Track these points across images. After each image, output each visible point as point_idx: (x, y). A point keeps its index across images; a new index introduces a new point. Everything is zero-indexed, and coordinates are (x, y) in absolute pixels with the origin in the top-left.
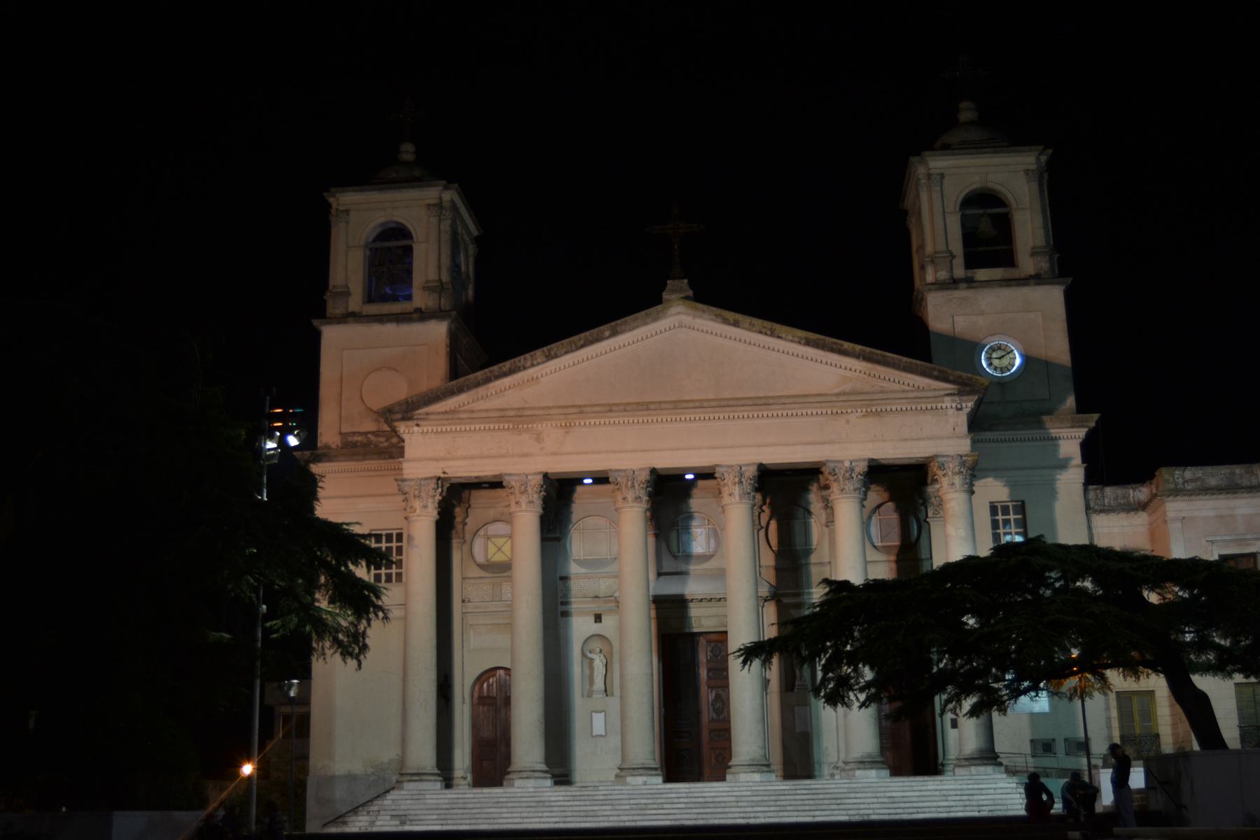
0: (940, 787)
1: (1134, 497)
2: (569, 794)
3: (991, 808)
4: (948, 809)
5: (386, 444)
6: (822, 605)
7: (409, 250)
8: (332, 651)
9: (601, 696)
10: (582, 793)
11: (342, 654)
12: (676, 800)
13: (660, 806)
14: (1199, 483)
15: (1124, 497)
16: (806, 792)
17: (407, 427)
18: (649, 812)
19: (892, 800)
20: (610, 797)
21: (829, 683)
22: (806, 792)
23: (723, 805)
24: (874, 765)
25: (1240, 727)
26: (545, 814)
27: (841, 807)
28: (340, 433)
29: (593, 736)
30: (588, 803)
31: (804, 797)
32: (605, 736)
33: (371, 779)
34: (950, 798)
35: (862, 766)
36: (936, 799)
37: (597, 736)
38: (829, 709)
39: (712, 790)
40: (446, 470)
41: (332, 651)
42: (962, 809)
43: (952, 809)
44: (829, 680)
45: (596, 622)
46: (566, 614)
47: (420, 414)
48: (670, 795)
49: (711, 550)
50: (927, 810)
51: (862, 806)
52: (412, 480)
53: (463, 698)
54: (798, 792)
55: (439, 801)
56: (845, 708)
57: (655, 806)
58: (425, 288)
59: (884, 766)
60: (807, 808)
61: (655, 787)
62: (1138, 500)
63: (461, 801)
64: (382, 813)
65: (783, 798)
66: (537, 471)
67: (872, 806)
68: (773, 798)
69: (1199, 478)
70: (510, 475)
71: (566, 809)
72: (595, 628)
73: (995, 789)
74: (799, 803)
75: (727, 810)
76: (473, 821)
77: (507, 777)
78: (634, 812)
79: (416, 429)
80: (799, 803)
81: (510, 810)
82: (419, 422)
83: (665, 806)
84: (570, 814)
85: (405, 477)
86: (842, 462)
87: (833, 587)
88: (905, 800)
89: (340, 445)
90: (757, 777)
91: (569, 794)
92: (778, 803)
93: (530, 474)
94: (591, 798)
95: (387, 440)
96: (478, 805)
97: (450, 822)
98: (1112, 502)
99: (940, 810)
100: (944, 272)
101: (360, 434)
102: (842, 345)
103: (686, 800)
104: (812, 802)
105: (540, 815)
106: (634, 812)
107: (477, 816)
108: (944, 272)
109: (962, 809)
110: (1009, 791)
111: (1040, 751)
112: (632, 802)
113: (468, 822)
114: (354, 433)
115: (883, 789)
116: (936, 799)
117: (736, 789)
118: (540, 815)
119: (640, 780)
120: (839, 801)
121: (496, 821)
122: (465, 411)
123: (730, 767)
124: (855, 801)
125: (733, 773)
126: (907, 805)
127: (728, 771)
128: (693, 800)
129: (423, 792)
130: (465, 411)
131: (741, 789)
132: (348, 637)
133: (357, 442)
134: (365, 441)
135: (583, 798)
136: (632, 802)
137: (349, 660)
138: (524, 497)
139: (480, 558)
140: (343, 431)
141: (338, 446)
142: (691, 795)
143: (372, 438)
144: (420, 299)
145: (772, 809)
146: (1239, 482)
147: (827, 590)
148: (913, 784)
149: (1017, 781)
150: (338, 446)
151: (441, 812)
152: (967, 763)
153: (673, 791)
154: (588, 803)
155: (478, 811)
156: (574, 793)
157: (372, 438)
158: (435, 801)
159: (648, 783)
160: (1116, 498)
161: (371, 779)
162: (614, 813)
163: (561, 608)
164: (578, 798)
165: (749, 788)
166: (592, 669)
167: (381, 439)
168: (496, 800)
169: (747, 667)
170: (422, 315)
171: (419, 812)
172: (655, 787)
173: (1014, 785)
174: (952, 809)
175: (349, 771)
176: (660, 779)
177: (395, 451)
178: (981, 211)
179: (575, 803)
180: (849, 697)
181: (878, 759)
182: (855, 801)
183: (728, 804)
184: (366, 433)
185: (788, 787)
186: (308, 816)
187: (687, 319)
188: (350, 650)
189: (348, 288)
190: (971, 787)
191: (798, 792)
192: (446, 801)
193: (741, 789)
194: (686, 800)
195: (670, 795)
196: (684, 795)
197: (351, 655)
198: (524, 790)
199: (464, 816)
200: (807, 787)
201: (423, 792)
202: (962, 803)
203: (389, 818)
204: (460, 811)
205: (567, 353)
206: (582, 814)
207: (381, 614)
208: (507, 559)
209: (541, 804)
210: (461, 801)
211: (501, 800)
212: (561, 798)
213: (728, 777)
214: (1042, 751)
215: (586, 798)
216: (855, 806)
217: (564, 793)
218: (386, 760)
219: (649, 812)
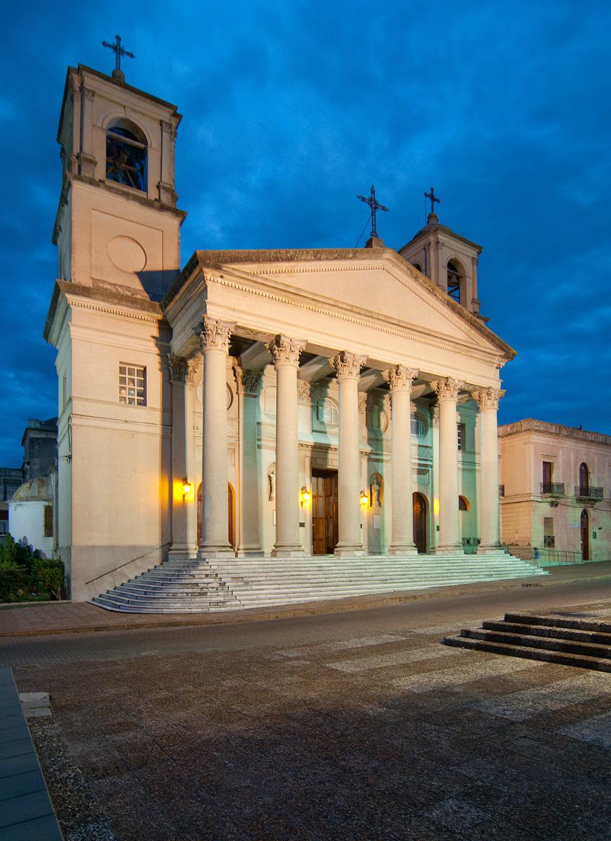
17: (213, 275)
46: (259, 447)
47: (228, 267)
70: (285, 337)
79: (220, 280)
82: (224, 275)
93: (297, 340)
95: (133, 295)
101: (110, 284)
102: (463, 311)
122: (262, 278)
130: (262, 278)
163: (258, 443)
187: (388, 265)
205: (327, 259)
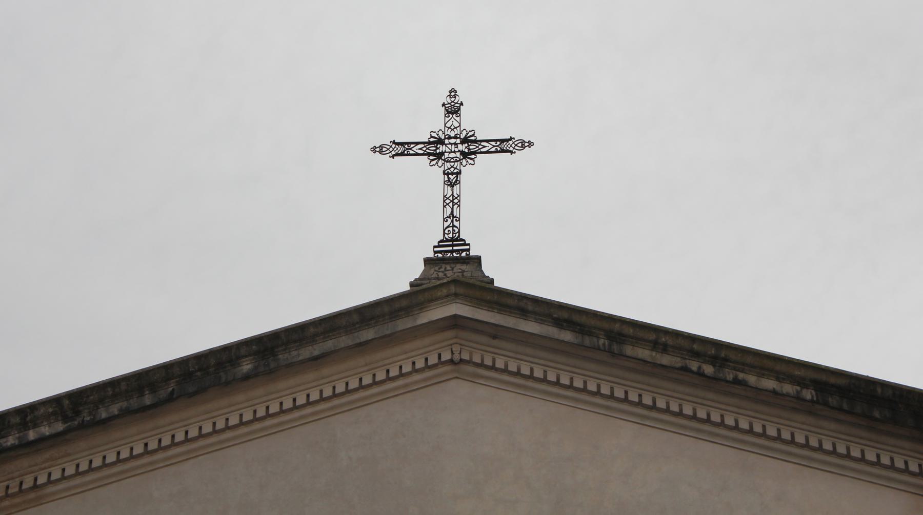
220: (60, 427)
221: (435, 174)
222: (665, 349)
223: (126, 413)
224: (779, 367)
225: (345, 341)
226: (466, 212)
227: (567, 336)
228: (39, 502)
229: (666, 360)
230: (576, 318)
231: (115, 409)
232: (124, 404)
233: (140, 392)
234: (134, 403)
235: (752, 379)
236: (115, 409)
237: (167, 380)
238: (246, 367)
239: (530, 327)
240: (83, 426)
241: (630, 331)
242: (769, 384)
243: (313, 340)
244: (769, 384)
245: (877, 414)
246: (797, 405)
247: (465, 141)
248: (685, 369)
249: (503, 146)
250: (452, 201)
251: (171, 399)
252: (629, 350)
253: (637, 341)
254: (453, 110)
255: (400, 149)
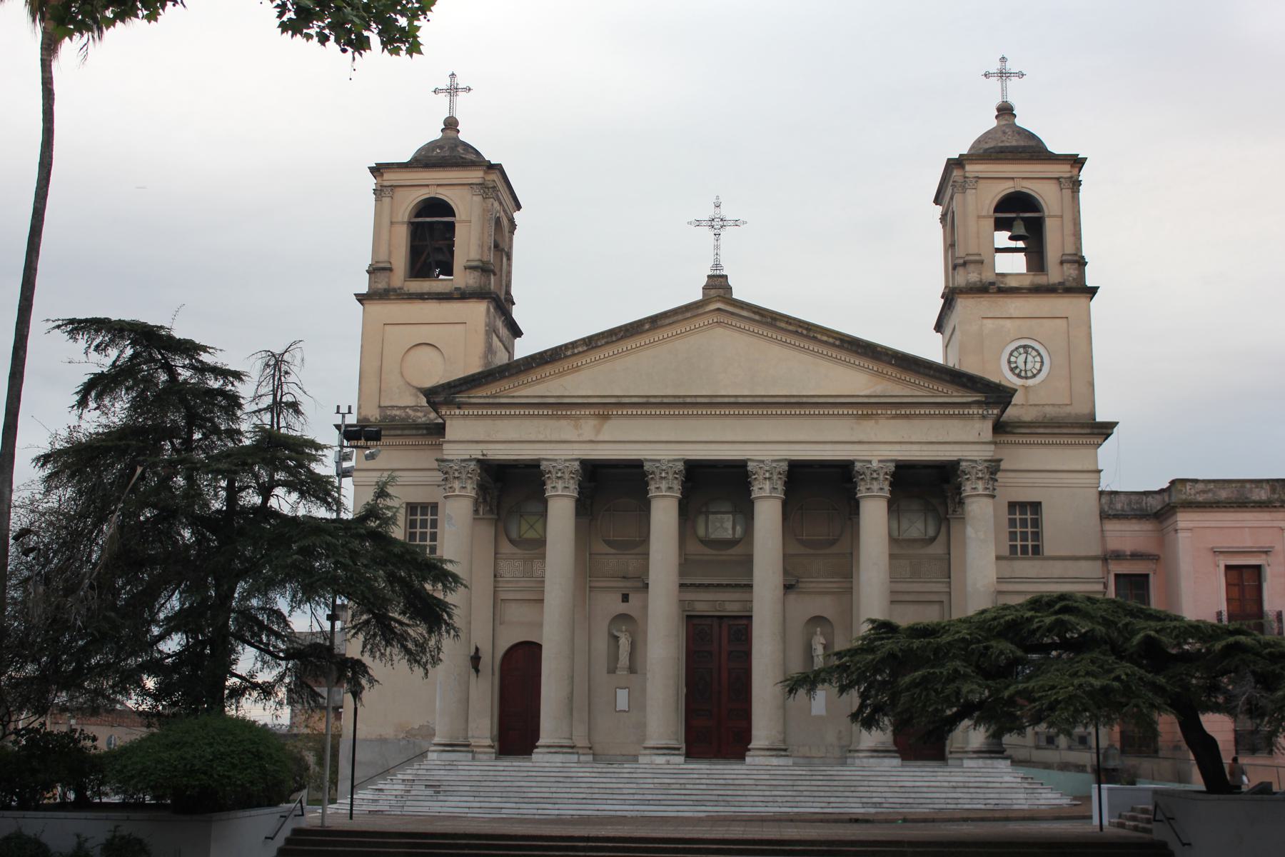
0: (949, 779)
1: (1146, 503)
2: (595, 770)
3: (997, 802)
4: (956, 801)
5: (423, 419)
6: (864, 638)
7: (451, 227)
8: (399, 657)
9: (625, 673)
10: (607, 770)
11: (408, 660)
12: (698, 781)
13: (683, 787)
14: (1210, 495)
15: (1137, 503)
16: (821, 778)
18: (672, 792)
19: (903, 790)
20: (635, 775)
21: (866, 709)
22: (821, 778)
23: (742, 787)
24: (886, 754)
25: (1235, 731)
26: (573, 790)
27: (855, 794)
28: (380, 407)
29: (616, 711)
30: (614, 780)
31: (820, 783)
32: (627, 712)
33: (401, 743)
34: (958, 790)
35: (875, 754)
36: (946, 790)
37: (620, 711)
38: (864, 732)
39: (732, 772)
40: (485, 452)
41: (399, 657)
42: (968, 801)
43: (960, 801)
44: (866, 707)
45: (623, 601)
48: (691, 776)
49: (736, 536)
50: (936, 801)
51: (874, 795)
52: (452, 461)
53: (493, 669)
54: (814, 778)
55: (472, 773)
56: (879, 731)
57: (678, 786)
58: (466, 268)
59: (897, 755)
60: (822, 794)
61: (677, 766)
62: (1151, 506)
63: (491, 773)
64: (416, 782)
65: (800, 783)
66: (574, 457)
67: (884, 795)
68: (790, 783)
69: (1210, 490)
71: (593, 785)
72: (622, 608)
73: (1001, 783)
74: (815, 788)
75: (747, 793)
76: (504, 795)
77: (536, 750)
78: (657, 792)
79: (457, 412)
80: (815, 788)
81: (539, 784)
83: (688, 786)
84: (596, 791)
85: (446, 457)
86: (870, 462)
87: (875, 625)
88: (916, 790)
89: (379, 418)
90: (775, 761)
91: (595, 770)
92: (795, 788)
94: (616, 775)
95: (425, 416)
96: (509, 779)
97: (482, 794)
98: (1125, 507)
99: (949, 801)
100: (975, 275)
103: (708, 781)
104: (827, 789)
105: (568, 790)
106: (657, 792)
107: (508, 789)
108: (975, 275)
109: (968, 801)
110: (1014, 785)
111: (1043, 743)
112: (656, 781)
113: (499, 794)
114: (393, 407)
115: (894, 779)
116: (946, 790)
117: (755, 772)
118: (568, 790)
119: (661, 760)
120: (853, 789)
121: (525, 795)
123: (749, 750)
124: (868, 789)
125: (753, 756)
126: (918, 795)
127: (748, 753)
128: (714, 781)
129: (455, 763)
131: (759, 772)
132: (416, 646)
133: (396, 416)
134: (403, 415)
135: (609, 775)
136: (656, 781)
137: (416, 667)
138: (560, 482)
139: (514, 535)
140: (382, 404)
141: (376, 419)
142: (711, 776)
143: (411, 412)
144: (461, 278)
145: (790, 793)
146: (1249, 495)
147: (870, 626)
148: (923, 774)
149: (1022, 775)
150: (376, 419)
151: (473, 784)
152: (975, 756)
153: (695, 772)
154: (614, 780)
155: (509, 784)
156: (600, 770)
157: (411, 412)
158: (467, 773)
159: (671, 762)
160: (1130, 503)
161: (401, 743)
162: (638, 791)
164: (605, 775)
165: (769, 772)
166: (618, 647)
167: (419, 414)
168: (525, 774)
169: (792, 695)
170: (463, 295)
171: (452, 783)
172: (677, 766)
173: (1019, 780)
174: (960, 801)
175: (381, 735)
176: (682, 759)
177: (439, 430)
178: (1013, 215)
179: (601, 780)
180: (883, 722)
181: (891, 749)
182: (868, 789)
183: (747, 788)
184: (405, 407)
185: (804, 773)
186: (340, 777)
188: (418, 658)
189: (391, 263)
190: (978, 779)
191: (814, 778)
192: (478, 773)
193: (759, 772)
194: (708, 781)
195: (691, 776)
196: (705, 776)
197: (418, 662)
198: (553, 765)
199: (496, 789)
200: (824, 773)
201: (455, 763)
202: (969, 796)
203: (423, 788)
204: (491, 784)
206: (608, 791)
207: (452, 632)
208: (539, 537)
209: (569, 780)
210: (491, 773)
211: (530, 774)
212: (588, 774)
213: (748, 760)
214: (1045, 744)
215: (612, 775)
216: (868, 794)
217: (591, 770)
218: (416, 727)
219: (672, 792)
220: (585, 348)
221: (710, 233)
222: (790, 324)
223: (607, 343)
224: (829, 333)
225: (680, 317)
226: (721, 252)
227: (757, 317)
228: (577, 371)
229: (791, 328)
230: (760, 311)
231: (603, 342)
232: (606, 340)
233: (611, 335)
234: (609, 339)
235: (819, 336)
236: (603, 342)
237: (620, 332)
238: (647, 326)
239: (745, 313)
240: (593, 348)
241: (778, 317)
242: (825, 338)
243: (669, 317)
244: (825, 338)
245: (859, 351)
246: (834, 345)
247: (722, 220)
248: (797, 331)
249: (736, 223)
250: (717, 247)
251: (622, 338)
252: (779, 324)
253: (781, 320)
254: (718, 206)
255: (698, 223)
